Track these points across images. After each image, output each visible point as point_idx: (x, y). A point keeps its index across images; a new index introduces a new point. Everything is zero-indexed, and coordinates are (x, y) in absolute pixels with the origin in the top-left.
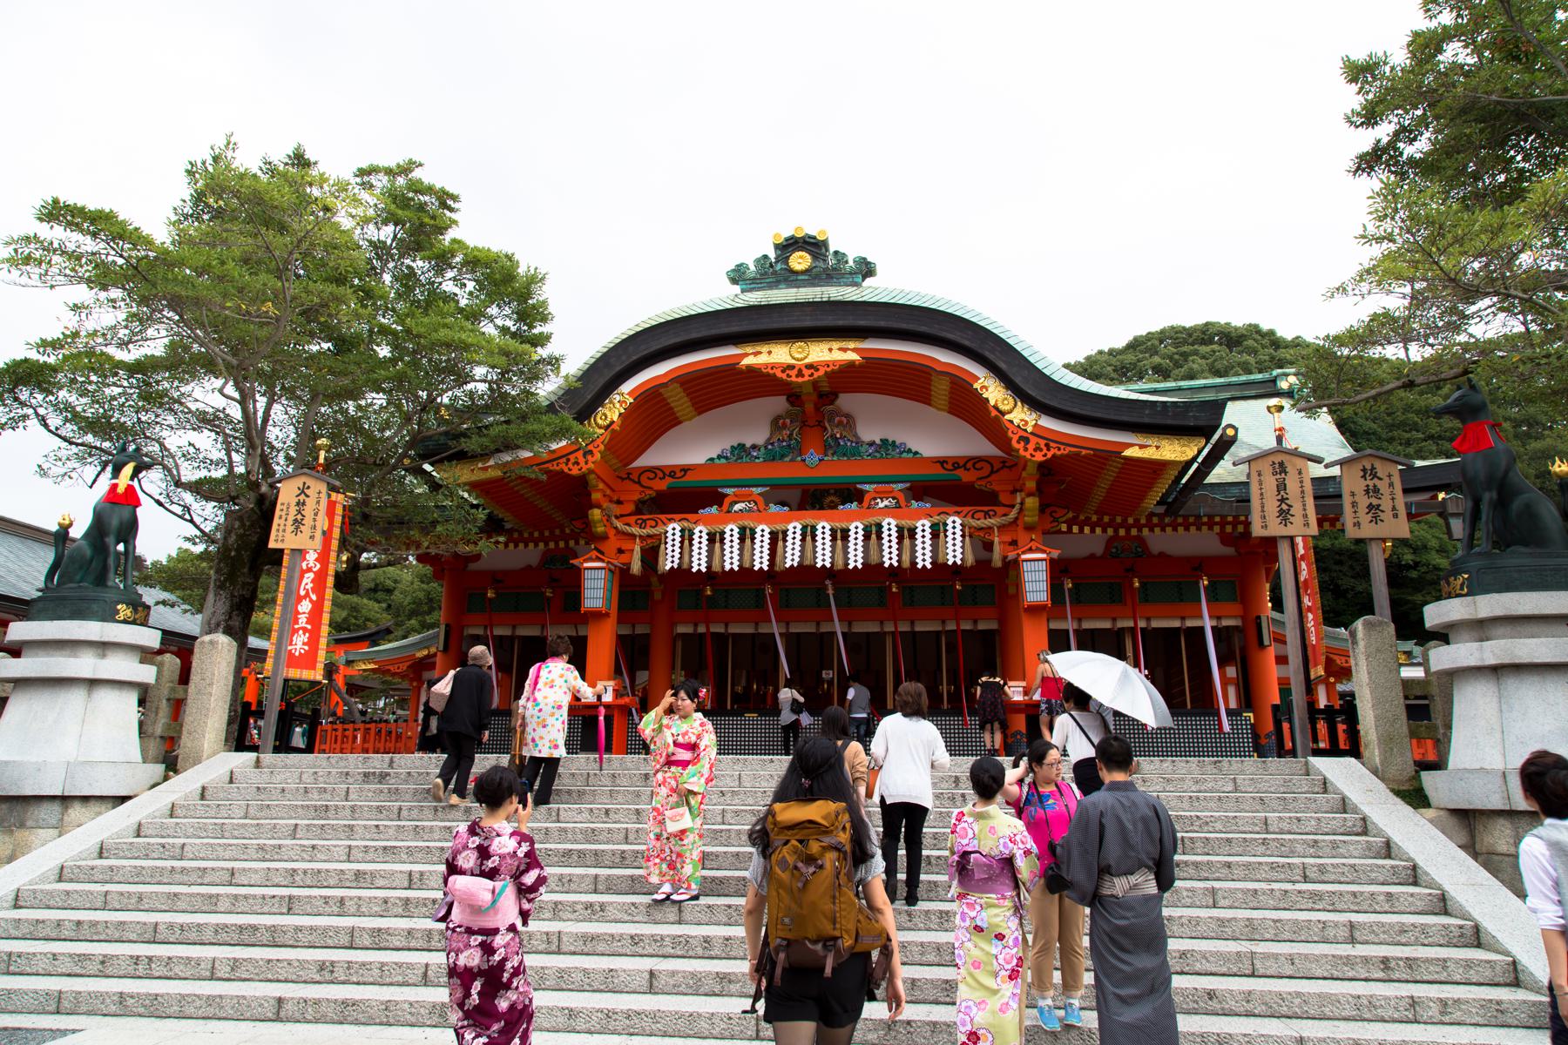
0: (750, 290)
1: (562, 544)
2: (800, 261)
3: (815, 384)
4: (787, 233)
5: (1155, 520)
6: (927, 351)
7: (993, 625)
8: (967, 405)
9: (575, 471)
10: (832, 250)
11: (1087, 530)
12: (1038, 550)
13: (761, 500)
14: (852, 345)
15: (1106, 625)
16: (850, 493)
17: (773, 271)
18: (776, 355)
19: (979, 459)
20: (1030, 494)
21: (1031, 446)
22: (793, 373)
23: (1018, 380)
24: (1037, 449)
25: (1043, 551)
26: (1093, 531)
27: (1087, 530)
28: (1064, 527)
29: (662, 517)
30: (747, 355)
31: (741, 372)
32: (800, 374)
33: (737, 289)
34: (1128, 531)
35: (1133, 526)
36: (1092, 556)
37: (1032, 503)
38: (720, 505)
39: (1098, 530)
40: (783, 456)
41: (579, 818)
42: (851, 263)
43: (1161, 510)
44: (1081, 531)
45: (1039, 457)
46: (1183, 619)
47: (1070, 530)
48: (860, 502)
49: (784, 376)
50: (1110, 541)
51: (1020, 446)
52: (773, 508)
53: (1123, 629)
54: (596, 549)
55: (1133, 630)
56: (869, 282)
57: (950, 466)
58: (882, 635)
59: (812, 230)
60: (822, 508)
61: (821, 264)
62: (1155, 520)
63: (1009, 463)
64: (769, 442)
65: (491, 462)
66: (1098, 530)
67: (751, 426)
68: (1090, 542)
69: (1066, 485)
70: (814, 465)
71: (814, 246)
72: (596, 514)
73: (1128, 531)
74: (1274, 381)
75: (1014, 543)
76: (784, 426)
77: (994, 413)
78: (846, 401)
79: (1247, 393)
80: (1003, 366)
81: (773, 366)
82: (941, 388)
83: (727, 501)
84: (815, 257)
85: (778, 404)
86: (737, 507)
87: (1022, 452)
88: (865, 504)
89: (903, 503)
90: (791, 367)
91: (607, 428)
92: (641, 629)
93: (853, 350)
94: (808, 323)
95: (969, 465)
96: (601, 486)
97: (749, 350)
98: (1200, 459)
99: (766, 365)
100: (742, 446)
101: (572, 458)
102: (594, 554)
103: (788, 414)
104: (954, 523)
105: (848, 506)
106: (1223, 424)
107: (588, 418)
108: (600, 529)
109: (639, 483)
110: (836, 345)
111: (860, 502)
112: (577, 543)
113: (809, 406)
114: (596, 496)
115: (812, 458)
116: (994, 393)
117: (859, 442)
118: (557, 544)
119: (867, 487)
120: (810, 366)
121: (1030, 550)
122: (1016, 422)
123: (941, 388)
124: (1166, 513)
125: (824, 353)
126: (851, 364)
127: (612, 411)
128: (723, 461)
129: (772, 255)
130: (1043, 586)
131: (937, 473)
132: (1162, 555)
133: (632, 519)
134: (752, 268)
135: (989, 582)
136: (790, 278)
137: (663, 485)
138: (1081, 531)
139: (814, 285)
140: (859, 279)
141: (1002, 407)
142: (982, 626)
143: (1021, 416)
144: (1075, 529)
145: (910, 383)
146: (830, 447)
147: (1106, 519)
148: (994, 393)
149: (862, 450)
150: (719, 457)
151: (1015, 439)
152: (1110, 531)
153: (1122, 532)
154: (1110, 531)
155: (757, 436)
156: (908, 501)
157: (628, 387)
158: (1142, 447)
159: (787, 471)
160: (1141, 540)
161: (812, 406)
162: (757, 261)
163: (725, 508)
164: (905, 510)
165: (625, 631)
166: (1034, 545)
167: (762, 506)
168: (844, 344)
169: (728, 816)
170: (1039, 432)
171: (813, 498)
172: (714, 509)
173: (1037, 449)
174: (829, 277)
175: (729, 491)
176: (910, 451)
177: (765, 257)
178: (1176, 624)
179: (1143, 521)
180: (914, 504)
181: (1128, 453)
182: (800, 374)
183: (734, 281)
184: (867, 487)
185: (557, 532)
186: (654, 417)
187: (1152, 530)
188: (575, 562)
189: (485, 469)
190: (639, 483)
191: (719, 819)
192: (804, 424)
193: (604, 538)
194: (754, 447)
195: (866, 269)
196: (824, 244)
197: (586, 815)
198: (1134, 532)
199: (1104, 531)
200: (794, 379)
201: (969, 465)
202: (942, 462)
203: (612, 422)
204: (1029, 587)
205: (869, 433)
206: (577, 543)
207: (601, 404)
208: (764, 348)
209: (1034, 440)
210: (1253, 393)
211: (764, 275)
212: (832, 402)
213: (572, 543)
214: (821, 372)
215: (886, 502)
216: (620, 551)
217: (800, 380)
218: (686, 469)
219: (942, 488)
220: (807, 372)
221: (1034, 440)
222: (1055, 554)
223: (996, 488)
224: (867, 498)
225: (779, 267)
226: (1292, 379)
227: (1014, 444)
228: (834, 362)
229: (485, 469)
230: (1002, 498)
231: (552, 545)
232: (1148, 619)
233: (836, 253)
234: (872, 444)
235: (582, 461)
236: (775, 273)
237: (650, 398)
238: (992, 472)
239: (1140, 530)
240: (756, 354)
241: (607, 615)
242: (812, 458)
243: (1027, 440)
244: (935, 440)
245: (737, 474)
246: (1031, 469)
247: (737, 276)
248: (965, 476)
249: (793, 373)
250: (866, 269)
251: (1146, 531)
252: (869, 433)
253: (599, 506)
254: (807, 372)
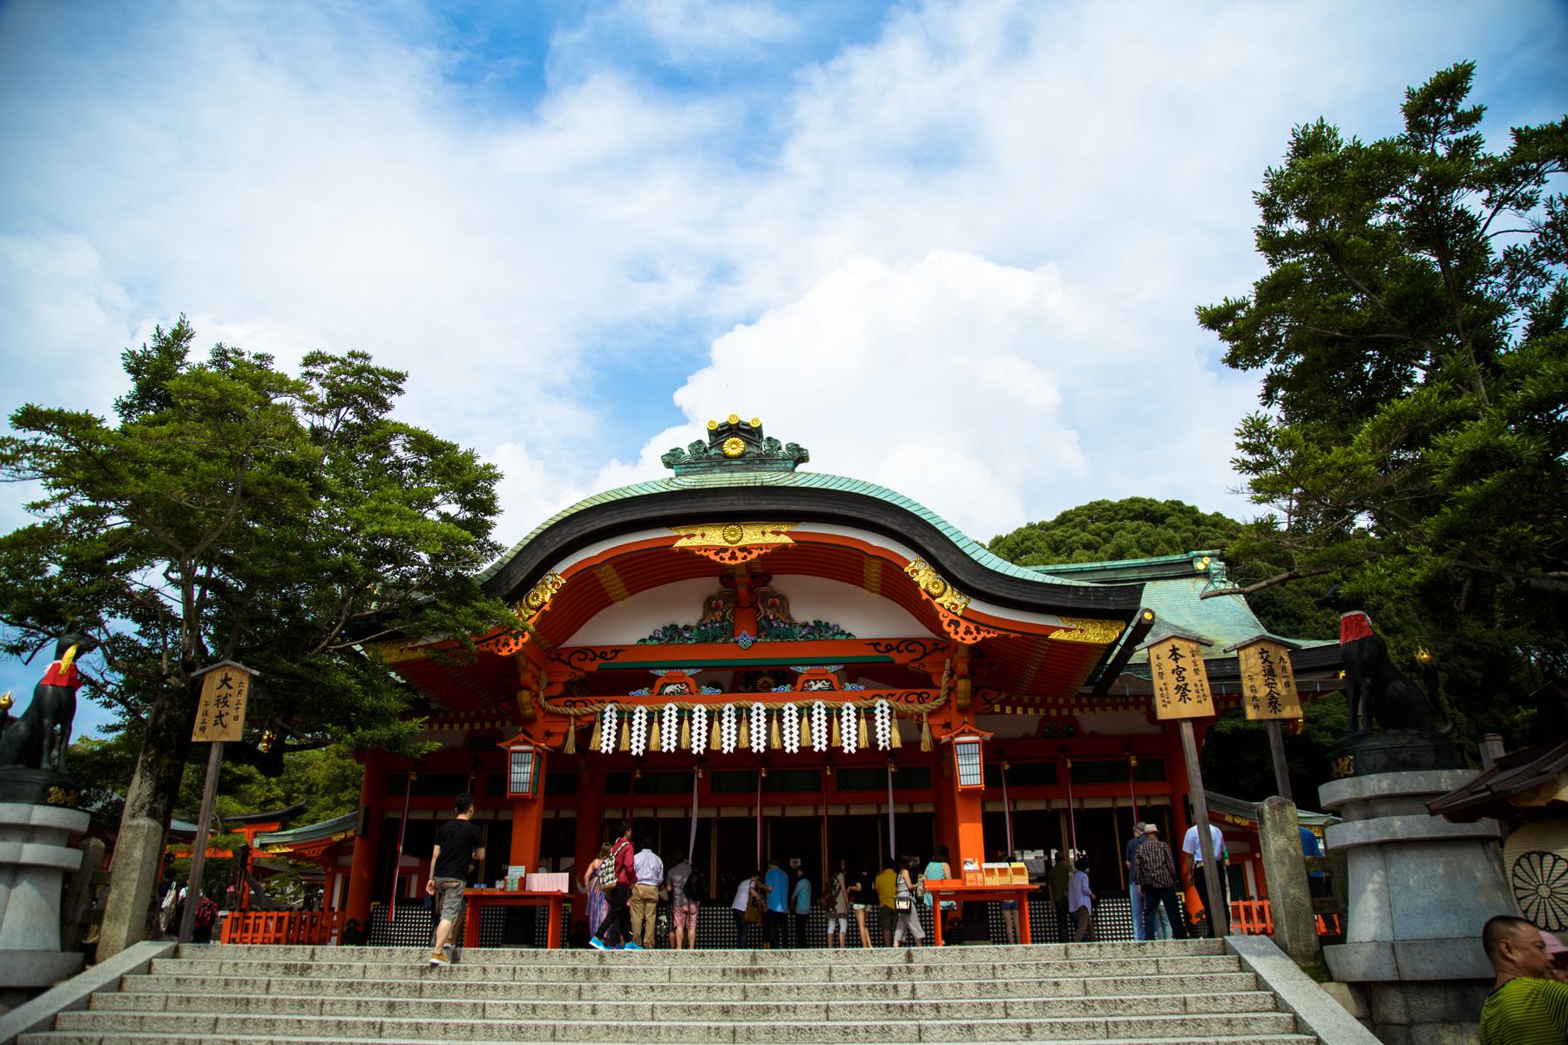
0: (685, 475)
1: (488, 725)
2: (733, 447)
3: (748, 565)
4: (721, 419)
5: (1084, 700)
6: (860, 535)
7: (930, 809)
8: (899, 589)
9: (505, 652)
10: (765, 436)
11: (1019, 711)
12: (970, 733)
13: (692, 682)
14: (785, 529)
15: (1040, 806)
16: (783, 676)
17: (706, 456)
18: (711, 538)
19: (907, 644)
20: (961, 677)
21: (962, 629)
22: (727, 555)
23: (947, 565)
24: (968, 632)
25: (976, 734)
26: (1025, 711)
27: (1019, 711)
28: (997, 708)
29: (592, 699)
30: (680, 537)
31: (674, 553)
32: (733, 557)
33: (671, 473)
34: (1059, 711)
35: (1064, 706)
36: (1026, 736)
37: (963, 685)
38: (652, 687)
39: (1031, 711)
40: (715, 638)
41: (506, 1014)
43: (1089, 690)
44: (1014, 711)
45: (969, 640)
46: (1114, 799)
47: (1003, 711)
48: (794, 684)
49: (717, 559)
50: (1042, 722)
51: (951, 630)
52: (706, 691)
53: (1057, 811)
54: (524, 732)
55: (1066, 811)
56: (801, 468)
57: (882, 648)
58: (815, 821)
59: (747, 417)
60: (755, 690)
61: (755, 450)
62: (1084, 700)
63: (942, 644)
64: (701, 623)
65: (421, 643)
66: (1031, 711)
67: (683, 608)
68: (1022, 721)
69: (998, 669)
70: (745, 646)
71: (750, 433)
72: (525, 696)
73: (1059, 711)
74: (1190, 562)
75: (947, 726)
76: (717, 607)
77: (925, 597)
78: (780, 583)
79: (1167, 573)
80: (931, 550)
81: (707, 549)
82: (873, 571)
83: (658, 683)
84: (748, 443)
85: (711, 585)
86: (669, 689)
87: (953, 636)
88: (799, 687)
89: (836, 686)
90: (725, 549)
91: (537, 609)
92: (566, 814)
93: (787, 533)
94: (741, 505)
95: (902, 647)
96: (531, 667)
97: (682, 533)
98: (1122, 642)
99: (700, 548)
100: (674, 627)
101: (502, 638)
102: (522, 737)
103: (721, 595)
104: (882, 706)
105: (781, 688)
106: (1144, 604)
107: (520, 599)
108: (529, 711)
109: (569, 664)
110: (769, 529)
111: (794, 684)
112: (503, 724)
113: (743, 590)
114: (525, 678)
115: (745, 639)
116: (924, 577)
117: (793, 624)
118: (482, 725)
119: (800, 669)
120: (742, 549)
121: (963, 733)
122: (946, 605)
123: (873, 571)
124: (1094, 694)
125: (756, 536)
126: (784, 547)
127: (545, 595)
128: (655, 642)
129: (707, 441)
130: (977, 769)
131: (870, 654)
132: (1093, 734)
133: (562, 701)
134: (687, 452)
135: (923, 768)
136: (724, 462)
137: (592, 666)
138: (1014, 711)
139: (747, 470)
140: (790, 465)
141: (934, 591)
142: (918, 809)
143: (950, 600)
144: (1008, 710)
145: (843, 566)
146: (763, 629)
147: (1037, 700)
148: (924, 577)
149: (796, 631)
150: (651, 638)
151: (946, 622)
152: (1042, 712)
153: (1053, 712)
154: (1042, 712)
155: (689, 616)
156: (842, 684)
157: (561, 568)
158: (1067, 630)
159: (718, 653)
160: (1072, 720)
161: (746, 590)
162: (692, 446)
163: (657, 689)
164: (838, 693)
165: (551, 815)
166: (967, 727)
167: (694, 688)
168: (776, 528)
169: (658, 1011)
170: (968, 615)
171: (747, 680)
172: (645, 692)
173: (968, 632)
174: (763, 462)
175: (660, 673)
176: (843, 633)
177: (700, 442)
178: (1108, 804)
179: (1073, 701)
180: (848, 686)
181: (1055, 636)
182: (733, 557)
183: (669, 465)
184: (800, 669)
185: (484, 712)
186: (585, 597)
187: (1082, 710)
188: (503, 745)
189: (415, 649)
190: (569, 664)
191: (648, 1015)
192: (737, 605)
193: (532, 720)
194: (687, 628)
195: (798, 455)
196: (759, 430)
197: (512, 1011)
198: (1065, 712)
199: (1036, 711)
200: (727, 561)
201: (902, 647)
202: (875, 643)
203: (544, 603)
204: (962, 770)
205: (803, 614)
206: (503, 724)
207: (534, 585)
208: (698, 532)
210: (1172, 573)
211: (699, 459)
212: (765, 584)
213: (498, 724)
214: (755, 554)
215: (819, 685)
216: (548, 734)
217: (733, 562)
218: (617, 650)
219: (875, 670)
220: (740, 555)
221: (964, 624)
222: (988, 736)
223: (929, 669)
224: (800, 681)
225: (713, 452)
226: (1206, 560)
227: (945, 626)
228: (767, 546)
229: (415, 649)
231: (477, 726)
232: (1081, 800)
233: (769, 439)
234: (805, 625)
235: (512, 642)
236: (709, 458)
237: (582, 580)
238: (925, 654)
239: (1071, 710)
240: (690, 536)
241: (534, 800)
242: (745, 639)
243: (957, 624)
244: (867, 622)
245: (669, 655)
246: (962, 652)
247: (672, 459)
248: (900, 658)
249: (727, 555)
250: (798, 455)
251: (1076, 712)
252: (803, 614)
253: (528, 688)
254: (740, 555)
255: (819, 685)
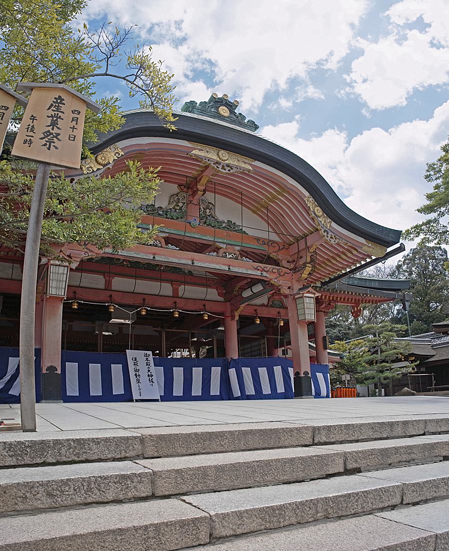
2: (224, 111)
42: (246, 121)
71: (232, 106)
91: (104, 166)
93: (249, 164)
119: (222, 245)
120: (228, 166)
131: (255, 246)
143: (324, 221)
184: (222, 245)
200: (220, 169)
209: (330, 233)
215: (231, 256)
230: (284, 263)
233: (240, 114)
240: (200, 150)
254: (226, 167)
255: (231, 256)
